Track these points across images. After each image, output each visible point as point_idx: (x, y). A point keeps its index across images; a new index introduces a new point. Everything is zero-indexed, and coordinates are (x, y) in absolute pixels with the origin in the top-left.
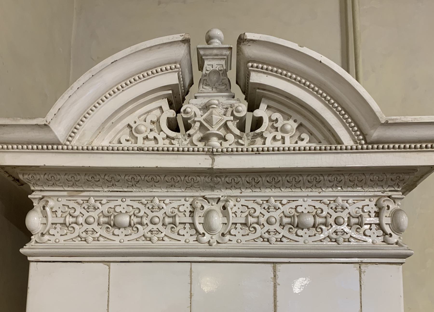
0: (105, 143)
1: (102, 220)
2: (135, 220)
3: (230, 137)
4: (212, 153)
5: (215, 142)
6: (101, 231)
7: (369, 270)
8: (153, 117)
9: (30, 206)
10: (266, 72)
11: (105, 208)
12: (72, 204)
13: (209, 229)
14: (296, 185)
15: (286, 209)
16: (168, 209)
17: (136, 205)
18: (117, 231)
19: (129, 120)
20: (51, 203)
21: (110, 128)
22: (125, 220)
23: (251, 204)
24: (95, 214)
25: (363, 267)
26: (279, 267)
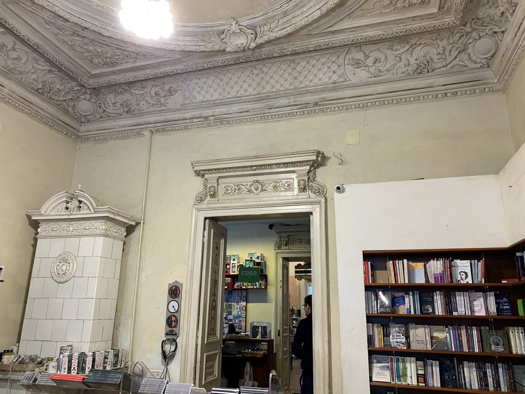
0: (53, 214)
1: (51, 229)
2: (57, 229)
3: (75, 211)
4: (68, 215)
5: (72, 212)
6: (51, 232)
7: (97, 238)
8: (62, 207)
9: (39, 227)
10: (80, 197)
11: (52, 227)
12: (46, 226)
13: (69, 231)
14: (87, 220)
15: (84, 226)
16: (63, 227)
17: (58, 226)
18: (53, 232)
19: (58, 208)
20: (43, 226)
21: (54, 210)
22: (55, 229)
23: (78, 225)
24: (50, 228)
25: (96, 237)
26: (81, 238)
